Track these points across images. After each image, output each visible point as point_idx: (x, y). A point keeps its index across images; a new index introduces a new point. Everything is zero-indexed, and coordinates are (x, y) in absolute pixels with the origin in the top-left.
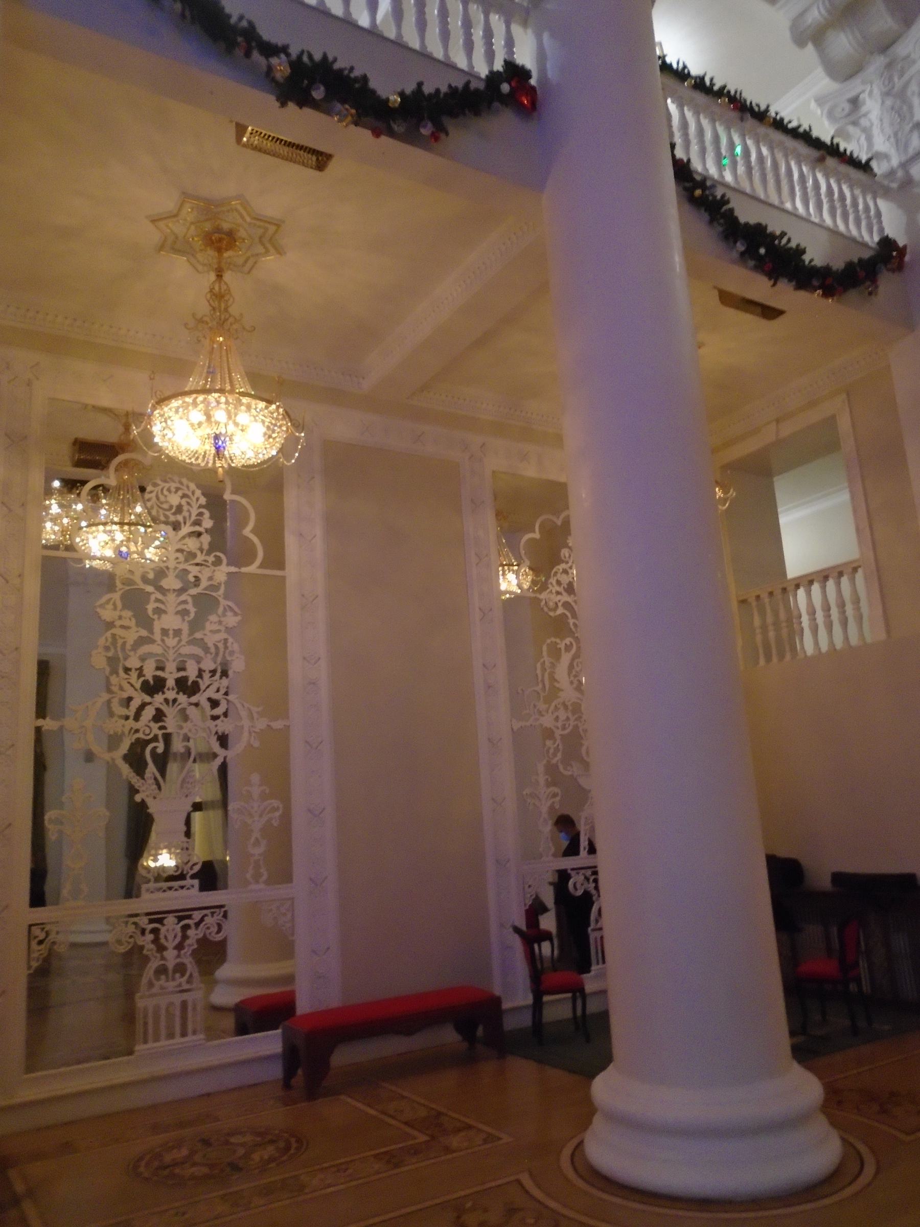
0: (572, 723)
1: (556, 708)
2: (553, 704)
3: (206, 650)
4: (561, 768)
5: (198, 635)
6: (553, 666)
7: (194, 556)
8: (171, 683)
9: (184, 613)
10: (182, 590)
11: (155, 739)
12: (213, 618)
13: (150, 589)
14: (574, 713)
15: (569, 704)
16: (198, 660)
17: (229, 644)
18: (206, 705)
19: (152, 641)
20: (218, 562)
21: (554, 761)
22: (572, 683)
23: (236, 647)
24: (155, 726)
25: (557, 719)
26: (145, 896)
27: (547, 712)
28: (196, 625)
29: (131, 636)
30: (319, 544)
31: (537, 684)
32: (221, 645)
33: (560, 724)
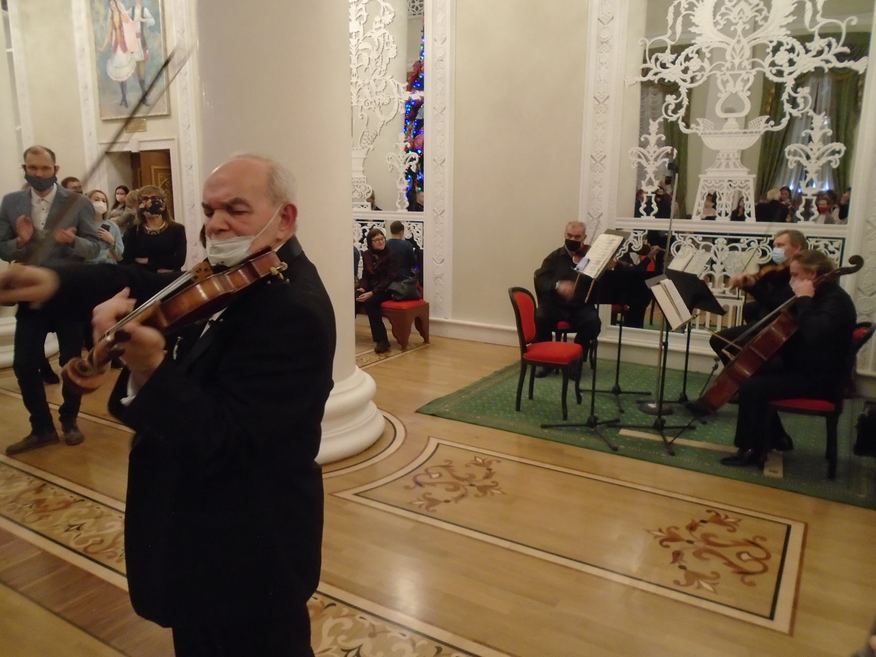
1: (687, 59)
2: (684, 54)
4: (682, 125)
6: (691, 6)
14: (711, 60)
15: (705, 51)
17: (386, 37)
21: (674, 118)
22: (716, 24)
25: (685, 71)
27: (673, 63)
32: (381, 39)
33: (688, 77)
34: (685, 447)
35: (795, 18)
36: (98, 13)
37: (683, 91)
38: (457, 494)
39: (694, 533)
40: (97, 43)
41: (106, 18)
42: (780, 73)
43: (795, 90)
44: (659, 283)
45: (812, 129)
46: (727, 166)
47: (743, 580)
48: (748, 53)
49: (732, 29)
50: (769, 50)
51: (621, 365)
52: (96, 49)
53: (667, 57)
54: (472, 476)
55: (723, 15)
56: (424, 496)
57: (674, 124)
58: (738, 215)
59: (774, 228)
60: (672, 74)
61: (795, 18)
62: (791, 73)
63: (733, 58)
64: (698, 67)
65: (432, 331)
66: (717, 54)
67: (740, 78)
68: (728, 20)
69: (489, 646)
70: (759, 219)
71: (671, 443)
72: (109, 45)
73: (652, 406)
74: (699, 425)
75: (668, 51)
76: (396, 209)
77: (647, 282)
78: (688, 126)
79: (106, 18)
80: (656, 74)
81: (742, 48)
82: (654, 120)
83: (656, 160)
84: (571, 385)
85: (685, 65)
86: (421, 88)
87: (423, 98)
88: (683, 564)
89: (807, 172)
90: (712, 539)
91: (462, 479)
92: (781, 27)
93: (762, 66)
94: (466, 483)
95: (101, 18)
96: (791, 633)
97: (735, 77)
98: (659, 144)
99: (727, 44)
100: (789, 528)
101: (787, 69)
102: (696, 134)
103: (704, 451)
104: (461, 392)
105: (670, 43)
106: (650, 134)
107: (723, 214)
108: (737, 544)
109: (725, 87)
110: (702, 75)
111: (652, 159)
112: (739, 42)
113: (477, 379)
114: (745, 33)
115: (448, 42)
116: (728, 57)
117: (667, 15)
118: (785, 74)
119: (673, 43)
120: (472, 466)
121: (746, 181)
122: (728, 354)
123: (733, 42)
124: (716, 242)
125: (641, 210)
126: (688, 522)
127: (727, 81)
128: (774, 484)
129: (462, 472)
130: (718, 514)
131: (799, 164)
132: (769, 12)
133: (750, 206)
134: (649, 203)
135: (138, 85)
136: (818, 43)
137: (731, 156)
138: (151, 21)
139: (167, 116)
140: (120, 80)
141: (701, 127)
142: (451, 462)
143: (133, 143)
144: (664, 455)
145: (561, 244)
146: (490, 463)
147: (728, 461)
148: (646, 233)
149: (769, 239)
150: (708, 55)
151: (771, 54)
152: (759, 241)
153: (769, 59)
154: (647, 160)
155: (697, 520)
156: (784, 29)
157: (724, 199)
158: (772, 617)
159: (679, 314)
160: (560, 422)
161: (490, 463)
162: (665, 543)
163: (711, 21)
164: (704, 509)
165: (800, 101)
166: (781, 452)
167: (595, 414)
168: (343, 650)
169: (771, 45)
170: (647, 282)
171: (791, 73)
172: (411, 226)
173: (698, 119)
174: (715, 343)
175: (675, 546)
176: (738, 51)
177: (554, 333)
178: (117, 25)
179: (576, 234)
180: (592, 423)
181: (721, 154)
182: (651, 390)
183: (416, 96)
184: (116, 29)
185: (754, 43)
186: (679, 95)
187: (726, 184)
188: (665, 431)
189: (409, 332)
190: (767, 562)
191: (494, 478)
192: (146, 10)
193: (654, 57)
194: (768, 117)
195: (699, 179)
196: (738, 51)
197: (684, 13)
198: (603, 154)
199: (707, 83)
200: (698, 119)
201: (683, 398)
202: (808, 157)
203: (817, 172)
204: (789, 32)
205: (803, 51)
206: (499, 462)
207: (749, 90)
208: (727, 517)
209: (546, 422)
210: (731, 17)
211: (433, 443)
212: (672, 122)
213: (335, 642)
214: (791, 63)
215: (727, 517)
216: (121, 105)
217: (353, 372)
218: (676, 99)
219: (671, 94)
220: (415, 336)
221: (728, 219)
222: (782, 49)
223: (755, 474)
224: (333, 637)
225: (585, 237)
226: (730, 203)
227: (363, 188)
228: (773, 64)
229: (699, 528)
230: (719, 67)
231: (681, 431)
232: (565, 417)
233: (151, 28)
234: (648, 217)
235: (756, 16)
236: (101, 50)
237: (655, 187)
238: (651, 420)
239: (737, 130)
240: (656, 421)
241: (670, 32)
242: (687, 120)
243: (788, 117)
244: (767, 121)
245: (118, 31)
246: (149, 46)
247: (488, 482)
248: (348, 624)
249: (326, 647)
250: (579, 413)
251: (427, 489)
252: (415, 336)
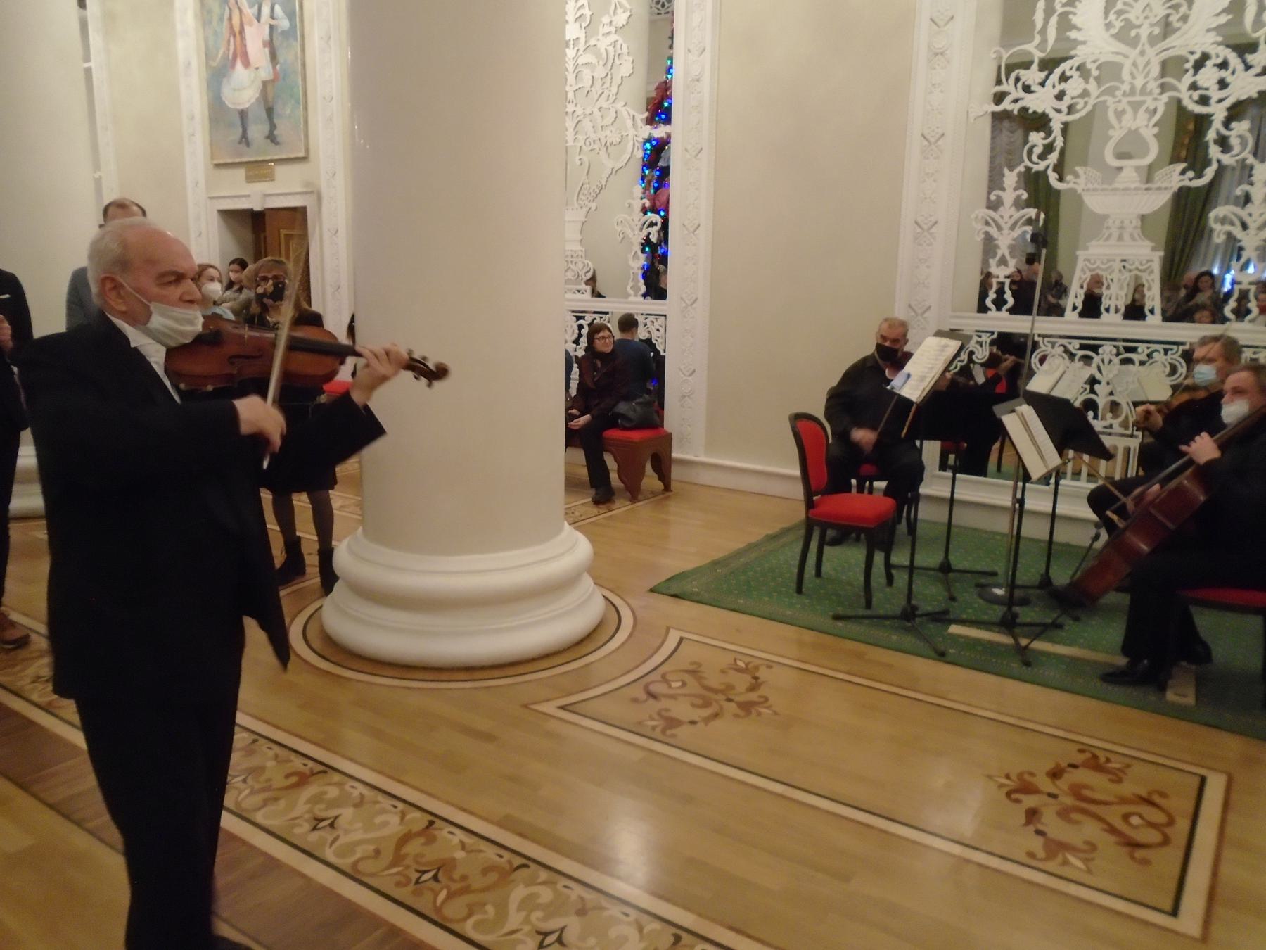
0: (1092, 101)
2: (1058, 71)
4: (1052, 177)
15: (1091, 67)
21: (1041, 166)
22: (1108, 26)
25: (1060, 96)
27: (1042, 84)
31: (1033, 39)
32: (611, 49)
33: (1063, 105)
34: (1048, 655)
35: (1230, 17)
36: (210, 12)
37: (1056, 126)
38: (706, 712)
39: (1058, 782)
40: (209, 55)
41: (221, 19)
42: (1204, 101)
43: (1227, 124)
44: (1013, 411)
45: (1251, 184)
46: (1120, 238)
47: (1133, 858)
48: (1156, 70)
49: (1133, 33)
50: (1189, 65)
51: (954, 530)
52: (208, 66)
53: (1032, 76)
54: (730, 687)
55: (1119, 13)
56: (659, 714)
57: (1042, 175)
58: (1135, 311)
59: (1189, 333)
60: (1040, 101)
61: (1230, 17)
62: (1220, 101)
63: (1133, 77)
64: (1080, 91)
65: (676, 473)
66: (1110, 71)
67: (1144, 107)
68: (1126, 20)
69: (749, 936)
70: (1166, 318)
71: (1026, 647)
72: (225, 57)
73: (999, 592)
74: (1068, 623)
75: (1035, 66)
76: (628, 295)
77: (997, 409)
78: (1061, 179)
79: (221, 19)
80: (1016, 101)
81: (1148, 63)
82: (1011, 169)
83: (1013, 228)
84: (879, 558)
85: (1059, 87)
86: (668, 121)
87: (669, 136)
88: (1040, 827)
89: (1241, 249)
90: (1087, 793)
91: (716, 691)
92: (1208, 30)
93: (1175, 89)
94: (721, 697)
95: (215, 19)
96: (1205, 937)
97: (1136, 106)
98: (1018, 204)
99: (1126, 57)
100: (1203, 780)
101: (1215, 94)
102: (1073, 191)
103: (1073, 662)
104: (715, 563)
105: (1038, 55)
106: (1003, 189)
107: (1112, 310)
108: (1123, 800)
109: (1120, 122)
110: (1086, 103)
111: (1006, 227)
112: (1142, 53)
113: (741, 546)
114: (1153, 41)
115: (707, 54)
116: (1125, 75)
117: (1033, 12)
118: (1213, 101)
119: (1042, 55)
120: (732, 672)
121: (1148, 261)
122: (1115, 517)
123: (1133, 53)
124: (1100, 351)
125: (988, 302)
126: (1050, 766)
127: (1124, 112)
128: (1180, 713)
129: (714, 681)
130: (1095, 757)
131: (1230, 236)
132: (1190, 7)
133: (1153, 298)
134: (1000, 292)
135: (264, 114)
137: (1126, 222)
138: (284, 24)
139: (304, 159)
140: (241, 107)
141: (1082, 180)
142: (700, 665)
143: (254, 196)
144: (1014, 665)
145: (869, 349)
146: (757, 668)
147: (1113, 677)
148: (995, 336)
149: (1181, 348)
150: (1095, 73)
151: (1191, 72)
152: (1166, 351)
153: (1188, 79)
154: (999, 228)
155: (1064, 764)
156: (1213, 34)
157: (1114, 287)
158: (1175, 912)
159: (1042, 457)
160: (861, 612)
161: (757, 668)
162: (1015, 796)
163: (1100, 22)
164: (1075, 747)
165: (1234, 141)
166: (1193, 667)
167: (914, 602)
168: (539, 933)
169: (1193, 58)
170: (997, 409)
171: (1220, 101)
172: (648, 321)
173: (1077, 169)
174: (1098, 500)
175: (1030, 801)
176: (1141, 68)
177: (854, 481)
178: (237, 29)
179: (893, 336)
180: (909, 614)
181: (1110, 221)
182: (996, 569)
183: (660, 132)
184: (235, 36)
185: (1165, 55)
186: (1049, 132)
187: (1117, 265)
188: (1017, 630)
189: (642, 474)
190: (1168, 831)
191: (763, 691)
192: (278, 8)
193: (1013, 76)
194: (1184, 165)
195: (1076, 257)
196: (1141, 68)
197: (1060, 10)
198: (933, 219)
199: (1091, 114)
200: (1077, 169)
201: (1046, 582)
202: (1245, 226)
203: (1257, 248)
204: (1220, 39)
205: (1241, 67)
206: (769, 667)
207: (1155, 125)
208: (1108, 760)
209: (840, 611)
210: (1131, 16)
211: (674, 637)
212: (1037, 173)
213: (527, 920)
214: (1223, 84)
215: (1108, 760)
216: (240, 142)
217: (561, 529)
218: (1045, 139)
219: (1038, 130)
220: (650, 480)
221: (1119, 317)
222: (1209, 63)
223: (1153, 698)
224: (524, 914)
225: (907, 341)
226: (1123, 293)
227: (580, 265)
228: (1194, 87)
229: (1066, 775)
230: (1111, 92)
231: (1042, 630)
232: (869, 605)
233: (283, 33)
234: (999, 314)
235: (1168, 16)
236: (214, 64)
237: (1010, 269)
238: (998, 612)
239: (1137, 185)
240: (1004, 617)
241: (1037, 39)
242: (1059, 168)
243: (1215, 166)
244: (1183, 172)
245: (238, 36)
246: (281, 58)
247: (753, 696)
248: (546, 895)
249: (514, 927)
250: (889, 600)
251: (665, 703)
252: (650, 480)
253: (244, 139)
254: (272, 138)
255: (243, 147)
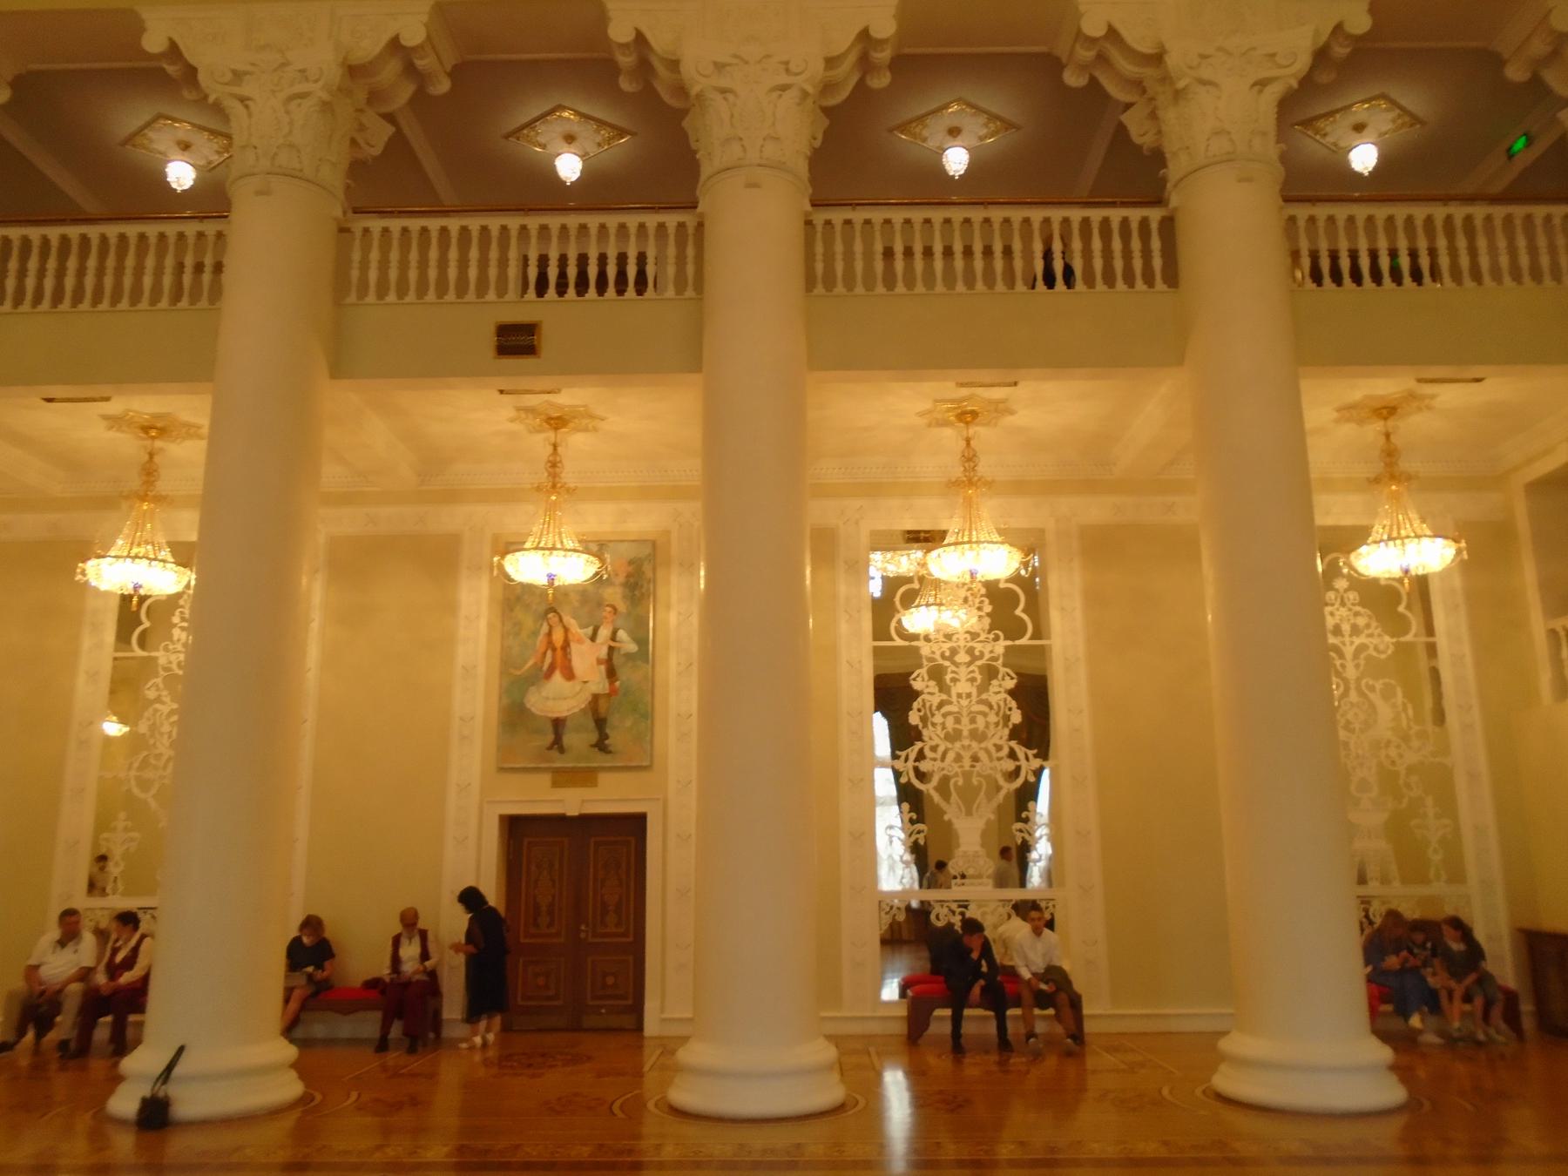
3: (991, 707)
5: (984, 696)
7: (978, 635)
8: (965, 733)
9: (973, 680)
10: (969, 664)
11: (956, 775)
12: (995, 682)
13: (947, 663)
16: (985, 715)
18: (993, 750)
19: (951, 703)
20: (997, 639)
23: (1014, 704)
24: (956, 766)
26: (954, 888)
28: (983, 688)
29: (935, 700)
30: (1078, 614)
42: (1393, 763)
79: (535, 633)
116: (1352, 746)
135: (592, 725)
136: (1415, 743)
138: (632, 647)
184: (554, 650)
192: (622, 634)
210: (1350, 716)
214: (1401, 756)
216: (550, 748)
253: (557, 744)
254: (601, 746)
255: (555, 753)
